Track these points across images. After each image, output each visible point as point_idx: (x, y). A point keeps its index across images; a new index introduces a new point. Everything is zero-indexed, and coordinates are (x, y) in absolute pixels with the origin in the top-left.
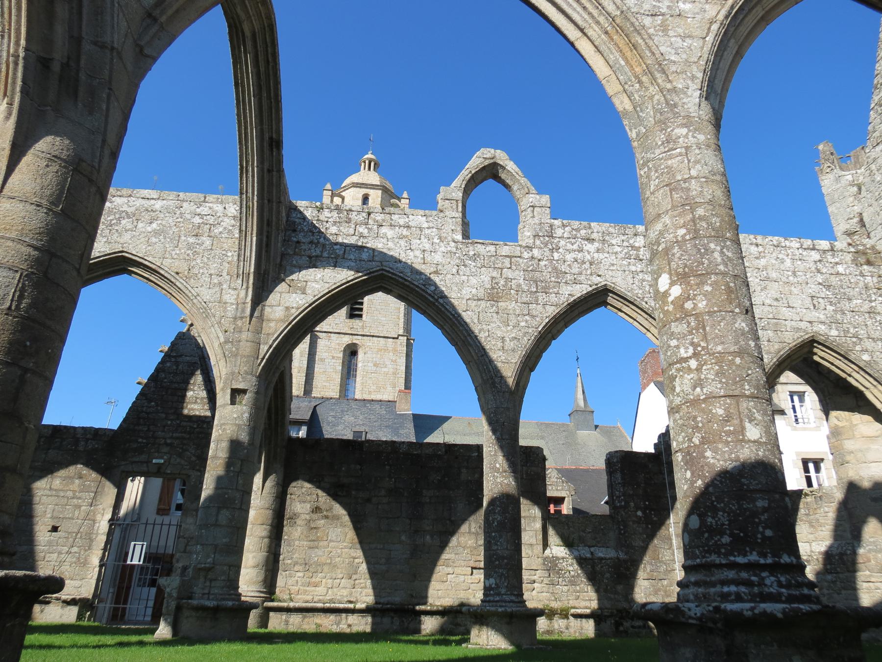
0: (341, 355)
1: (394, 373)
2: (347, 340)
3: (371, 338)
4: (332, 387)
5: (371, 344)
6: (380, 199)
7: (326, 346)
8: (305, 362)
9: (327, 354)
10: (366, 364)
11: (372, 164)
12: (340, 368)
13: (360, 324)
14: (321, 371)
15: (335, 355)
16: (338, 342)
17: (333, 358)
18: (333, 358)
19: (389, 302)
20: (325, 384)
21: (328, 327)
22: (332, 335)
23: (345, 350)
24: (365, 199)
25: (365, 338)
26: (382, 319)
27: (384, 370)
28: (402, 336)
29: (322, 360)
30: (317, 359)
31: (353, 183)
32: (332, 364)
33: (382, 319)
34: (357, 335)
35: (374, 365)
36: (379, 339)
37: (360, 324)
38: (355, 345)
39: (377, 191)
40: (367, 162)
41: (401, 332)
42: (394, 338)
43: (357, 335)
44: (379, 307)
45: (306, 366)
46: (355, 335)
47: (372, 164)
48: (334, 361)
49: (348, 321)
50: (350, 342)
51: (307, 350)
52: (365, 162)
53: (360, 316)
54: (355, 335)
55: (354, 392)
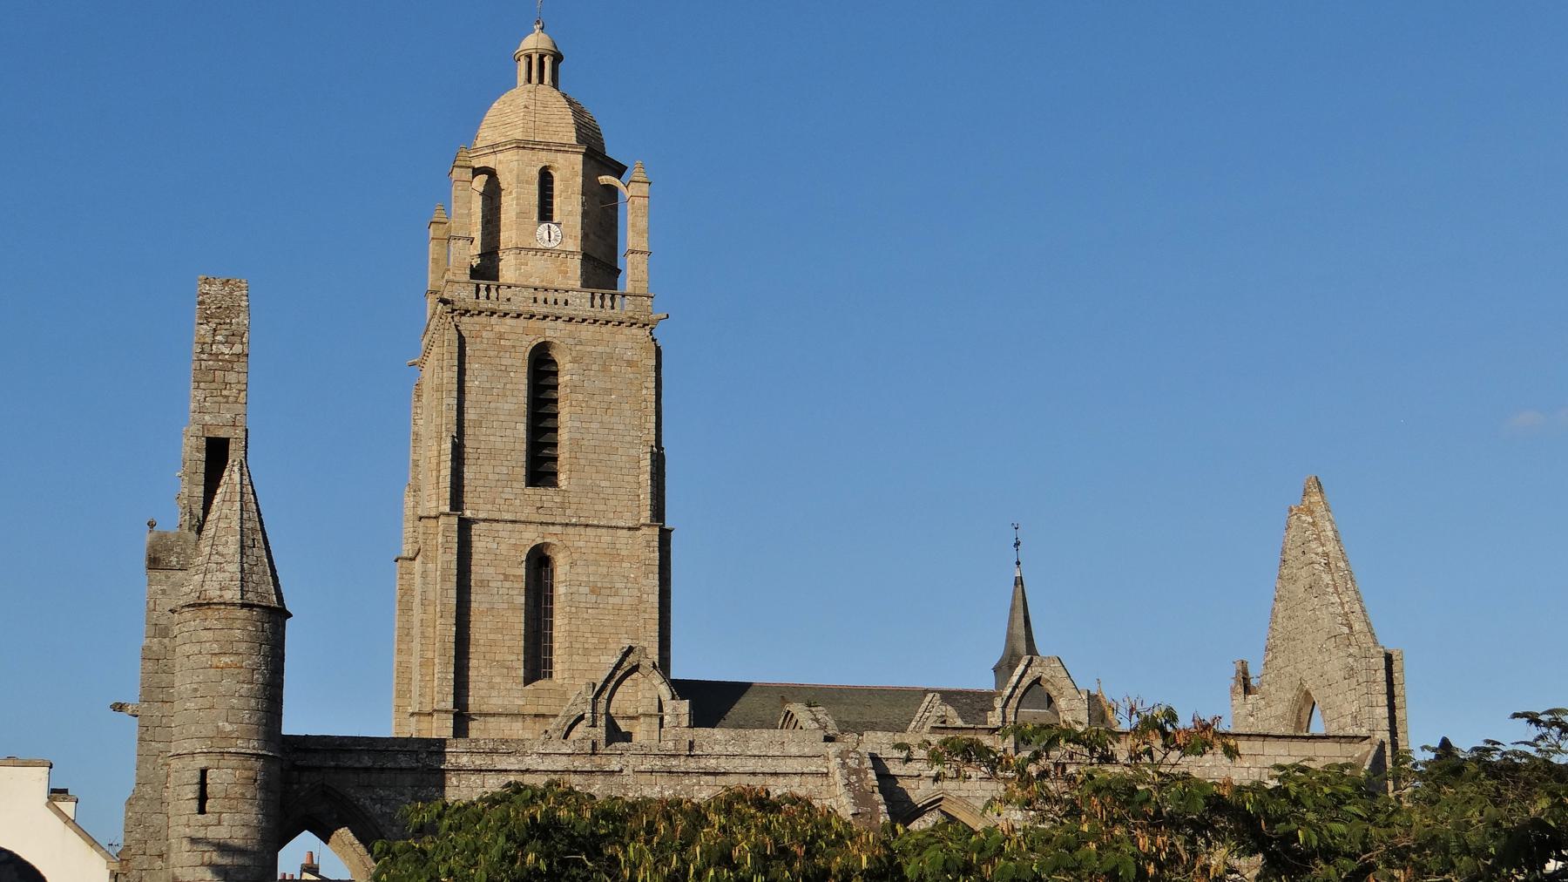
0: (522, 571)
1: (635, 608)
2: (531, 537)
3: (582, 530)
4: (508, 644)
5: (581, 544)
6: (580, 180)
7: (489, 551)
8: (453, 593)
9: (491, 570)
10: (574, 589)
11: (547, 61)
12: (522, 600)
13: (558, 499)
14: (484, 606)
15: (510, 571)
16: (513, 541)
17: (506, 577)
18: (506, 577)
19: (615, 445)
20: (491, 636)
21: (489, 507)
22: (499, 526)
23: (528, 560)
24: (546, 178)
25: (570, 530)
26: (603, 484)
27: (611, 600)
28: (649, 526)
29: (484, 583)
30: (472, 584)
31: (518, 141)
32: (505, 591)
33: (603, 484)
34: (553, 524)
35: (593, 592)
36: (600, 531)
37: (558, 499)
38: (545, 545)
39: (572, 156)
40: (535, 58)
41: (646, 516)
42: (630, 529)
43: (553, 524)
44: (595, 456)
45: (454, 601)
46: (547, 524)
47: (547, 61)
48: (507, 584)
49: (530, 490)
50: (539, 541)
51: (454, 565)
52: (529, 57)
53: (555, 474)
54: (547, 524)
55: (551, 648)
